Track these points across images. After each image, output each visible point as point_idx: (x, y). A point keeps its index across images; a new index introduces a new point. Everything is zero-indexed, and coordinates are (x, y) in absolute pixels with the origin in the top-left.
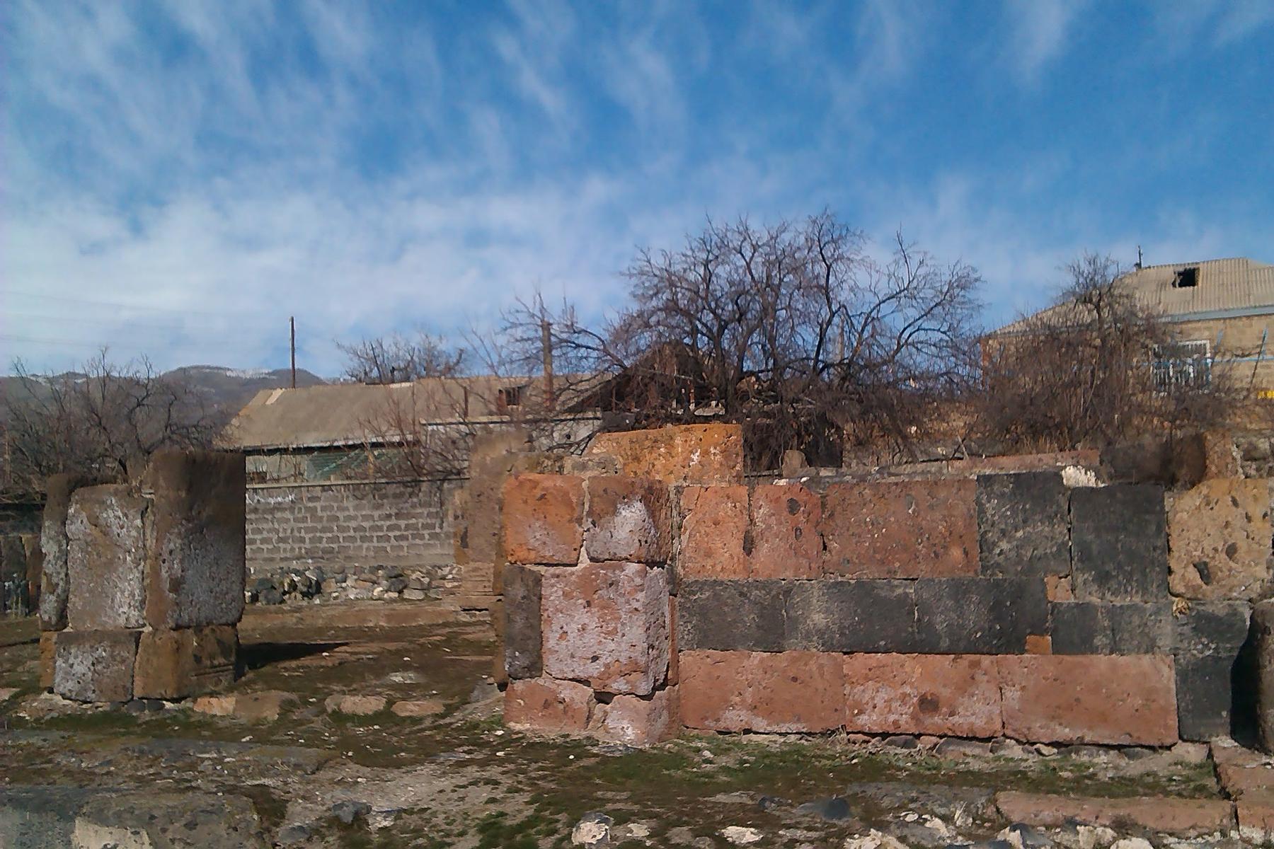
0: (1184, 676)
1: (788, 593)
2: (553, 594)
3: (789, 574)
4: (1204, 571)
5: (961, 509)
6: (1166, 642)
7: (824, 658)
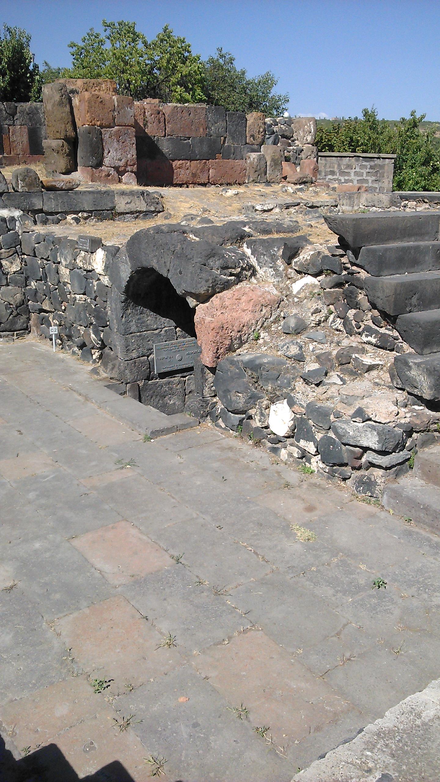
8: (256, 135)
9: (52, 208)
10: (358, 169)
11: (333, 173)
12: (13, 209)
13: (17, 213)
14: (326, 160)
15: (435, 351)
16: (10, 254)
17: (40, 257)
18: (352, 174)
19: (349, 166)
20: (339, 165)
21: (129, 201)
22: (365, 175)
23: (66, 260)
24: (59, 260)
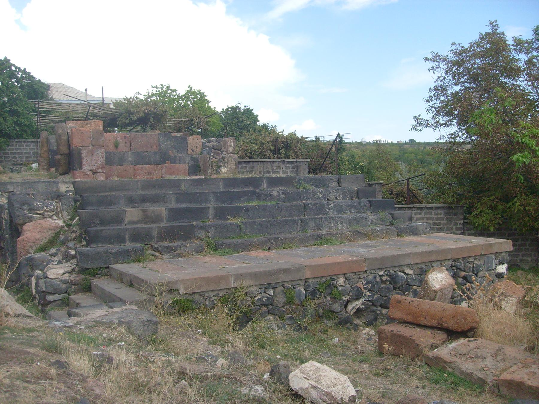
0: (189, 167)
1: (124, 154)
2: (84, 152)
3: (124, 151)
4: (193, 150)
6: (187, 162)
7: (131, 166)
10: (284, 169)
11: (268, 172)
14: (263, 164)
15: (100, 246)
18: (281, 173)
19: (279, 168)
20: (272, 167)
22: (289, 173)
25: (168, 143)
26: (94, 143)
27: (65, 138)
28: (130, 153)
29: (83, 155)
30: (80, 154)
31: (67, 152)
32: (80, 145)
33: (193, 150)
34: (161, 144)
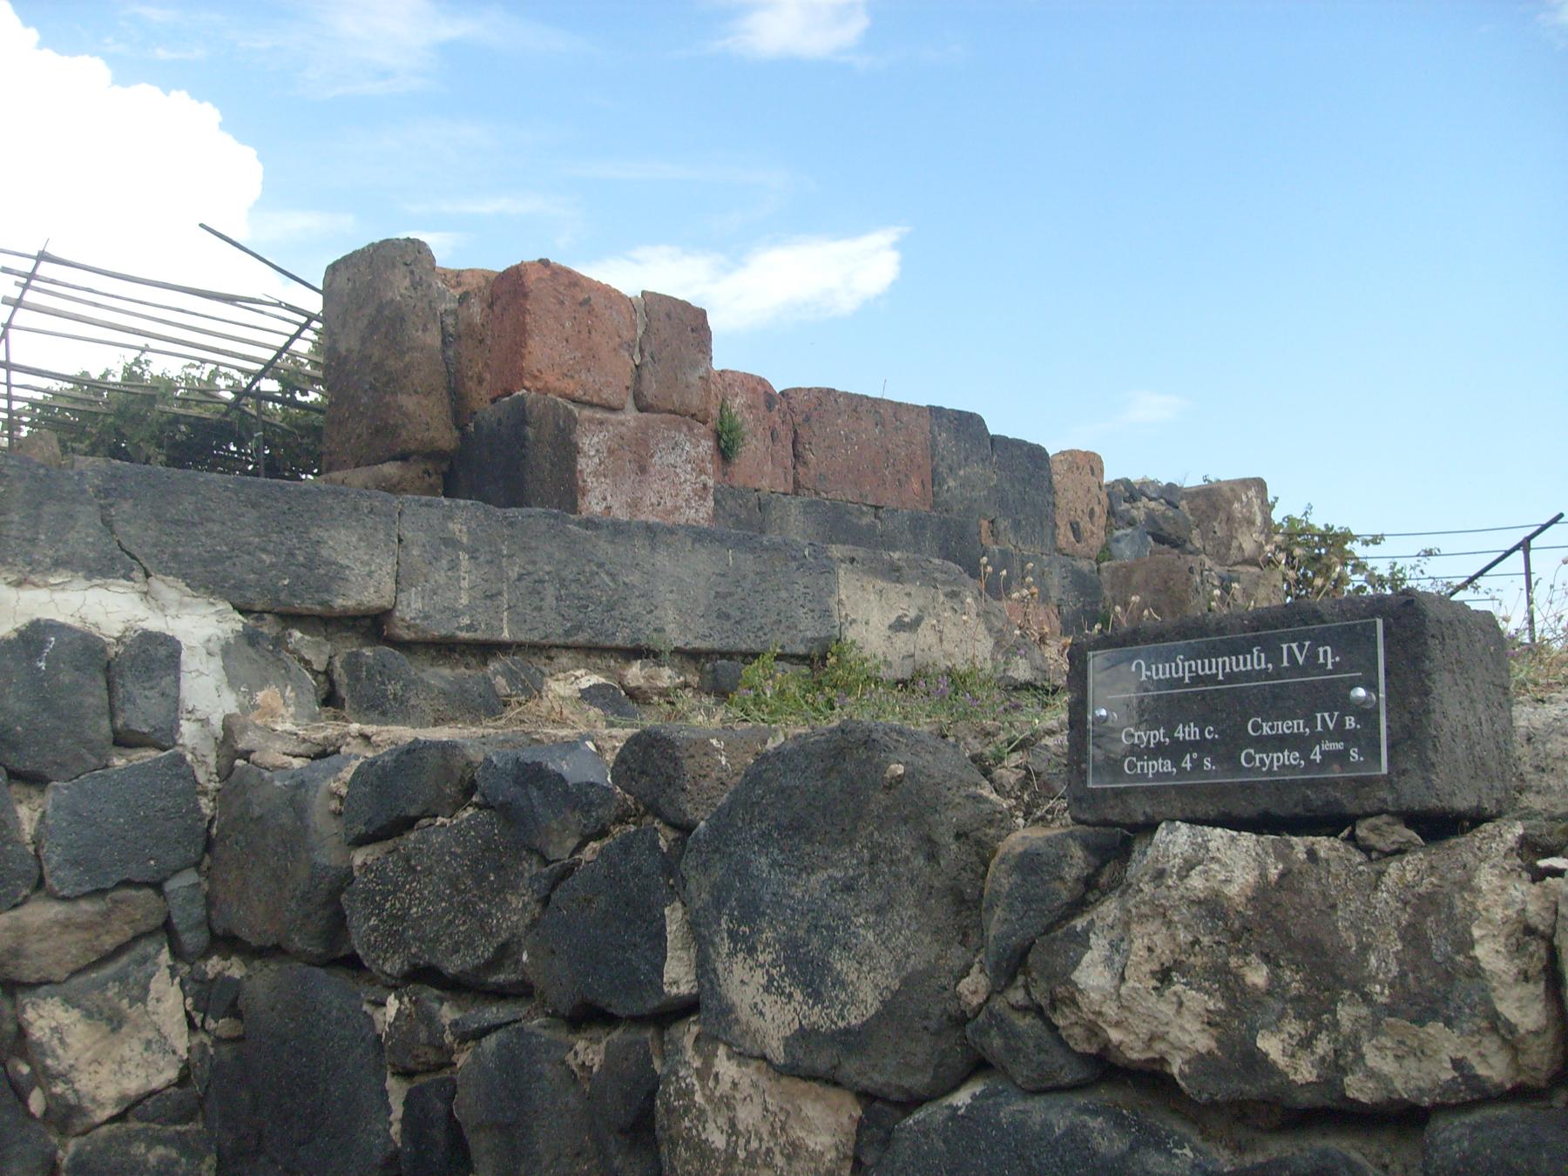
2: (591, 444)
3: (765, 484)
4: (1075, 529)
5: (919, 438)
6: (1055, 594)
8: (1085, 524)
9: (457, 614)
12: (169, 589)
13: (199, 625)
16: (109, 942)
17: (394, 965)
21: (913, 613)
23: (807, 973)
24: (678, 976)
25: (978, 469)
26: (651, 389)
27: (433, 339)
28: (794, 506)
29: (582, 463)
30: (568, 451)
31: (446, 438)
32: (569, 386)
33: (1075, 529)
34: (943, 469)
